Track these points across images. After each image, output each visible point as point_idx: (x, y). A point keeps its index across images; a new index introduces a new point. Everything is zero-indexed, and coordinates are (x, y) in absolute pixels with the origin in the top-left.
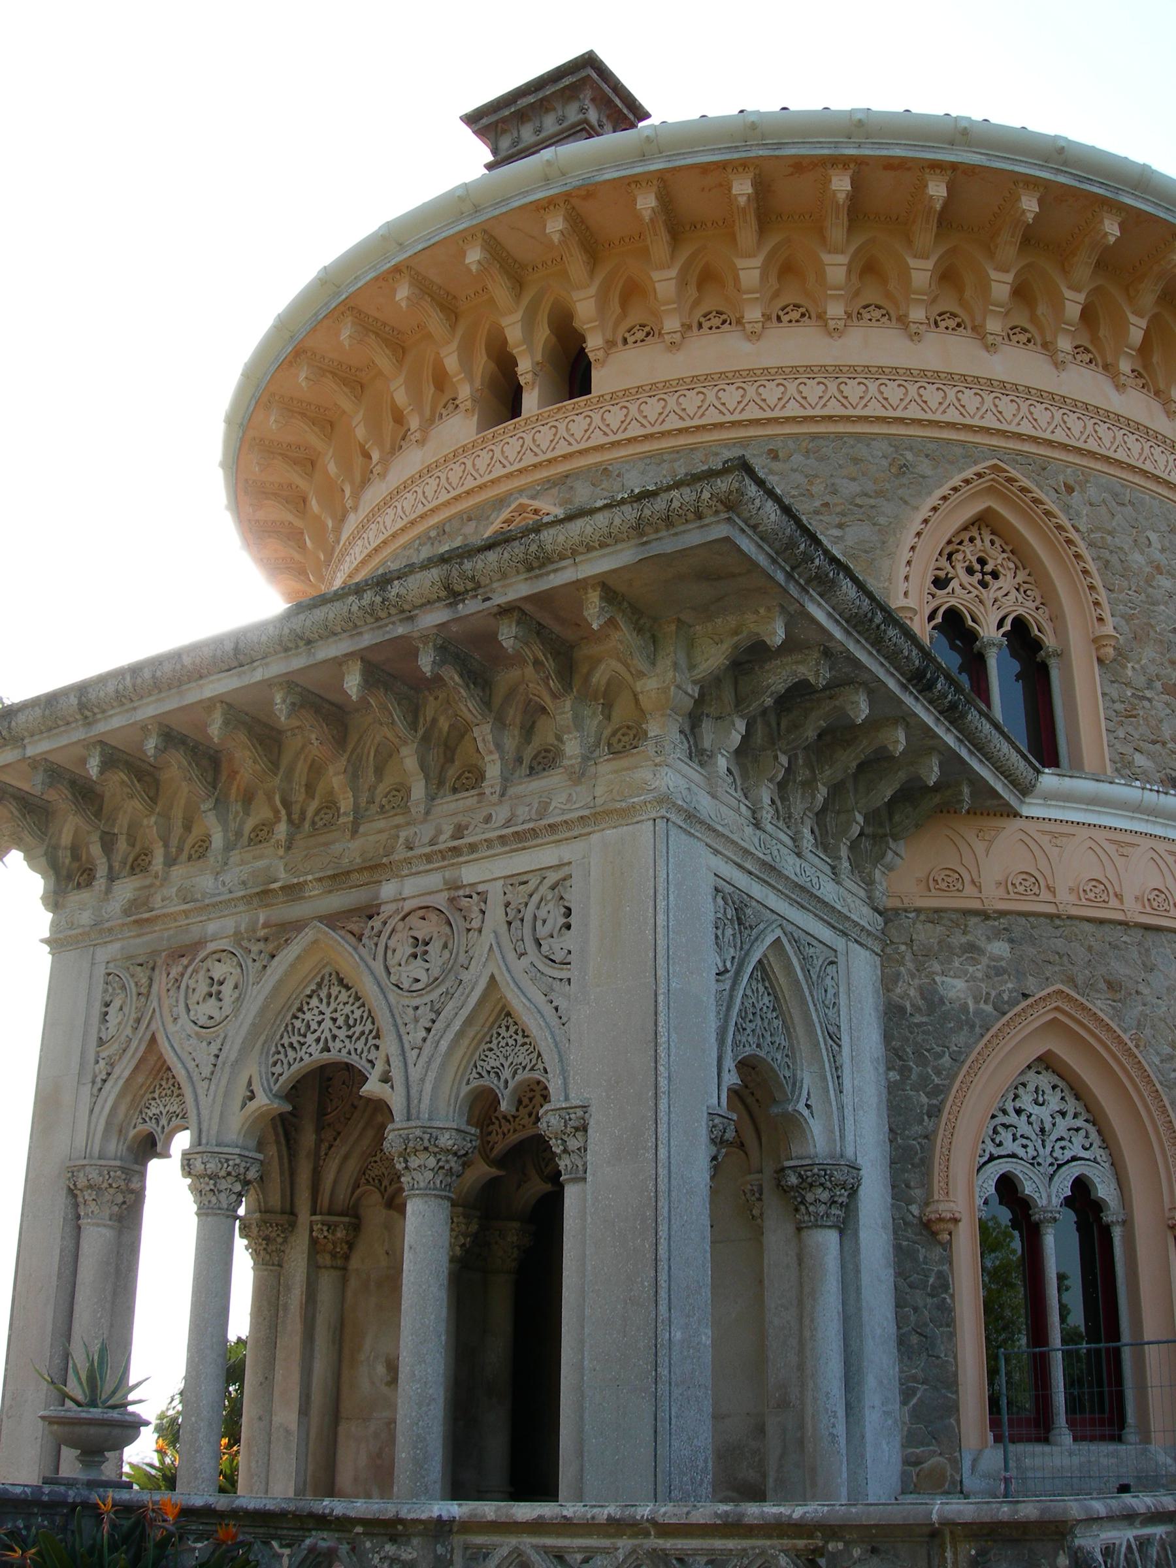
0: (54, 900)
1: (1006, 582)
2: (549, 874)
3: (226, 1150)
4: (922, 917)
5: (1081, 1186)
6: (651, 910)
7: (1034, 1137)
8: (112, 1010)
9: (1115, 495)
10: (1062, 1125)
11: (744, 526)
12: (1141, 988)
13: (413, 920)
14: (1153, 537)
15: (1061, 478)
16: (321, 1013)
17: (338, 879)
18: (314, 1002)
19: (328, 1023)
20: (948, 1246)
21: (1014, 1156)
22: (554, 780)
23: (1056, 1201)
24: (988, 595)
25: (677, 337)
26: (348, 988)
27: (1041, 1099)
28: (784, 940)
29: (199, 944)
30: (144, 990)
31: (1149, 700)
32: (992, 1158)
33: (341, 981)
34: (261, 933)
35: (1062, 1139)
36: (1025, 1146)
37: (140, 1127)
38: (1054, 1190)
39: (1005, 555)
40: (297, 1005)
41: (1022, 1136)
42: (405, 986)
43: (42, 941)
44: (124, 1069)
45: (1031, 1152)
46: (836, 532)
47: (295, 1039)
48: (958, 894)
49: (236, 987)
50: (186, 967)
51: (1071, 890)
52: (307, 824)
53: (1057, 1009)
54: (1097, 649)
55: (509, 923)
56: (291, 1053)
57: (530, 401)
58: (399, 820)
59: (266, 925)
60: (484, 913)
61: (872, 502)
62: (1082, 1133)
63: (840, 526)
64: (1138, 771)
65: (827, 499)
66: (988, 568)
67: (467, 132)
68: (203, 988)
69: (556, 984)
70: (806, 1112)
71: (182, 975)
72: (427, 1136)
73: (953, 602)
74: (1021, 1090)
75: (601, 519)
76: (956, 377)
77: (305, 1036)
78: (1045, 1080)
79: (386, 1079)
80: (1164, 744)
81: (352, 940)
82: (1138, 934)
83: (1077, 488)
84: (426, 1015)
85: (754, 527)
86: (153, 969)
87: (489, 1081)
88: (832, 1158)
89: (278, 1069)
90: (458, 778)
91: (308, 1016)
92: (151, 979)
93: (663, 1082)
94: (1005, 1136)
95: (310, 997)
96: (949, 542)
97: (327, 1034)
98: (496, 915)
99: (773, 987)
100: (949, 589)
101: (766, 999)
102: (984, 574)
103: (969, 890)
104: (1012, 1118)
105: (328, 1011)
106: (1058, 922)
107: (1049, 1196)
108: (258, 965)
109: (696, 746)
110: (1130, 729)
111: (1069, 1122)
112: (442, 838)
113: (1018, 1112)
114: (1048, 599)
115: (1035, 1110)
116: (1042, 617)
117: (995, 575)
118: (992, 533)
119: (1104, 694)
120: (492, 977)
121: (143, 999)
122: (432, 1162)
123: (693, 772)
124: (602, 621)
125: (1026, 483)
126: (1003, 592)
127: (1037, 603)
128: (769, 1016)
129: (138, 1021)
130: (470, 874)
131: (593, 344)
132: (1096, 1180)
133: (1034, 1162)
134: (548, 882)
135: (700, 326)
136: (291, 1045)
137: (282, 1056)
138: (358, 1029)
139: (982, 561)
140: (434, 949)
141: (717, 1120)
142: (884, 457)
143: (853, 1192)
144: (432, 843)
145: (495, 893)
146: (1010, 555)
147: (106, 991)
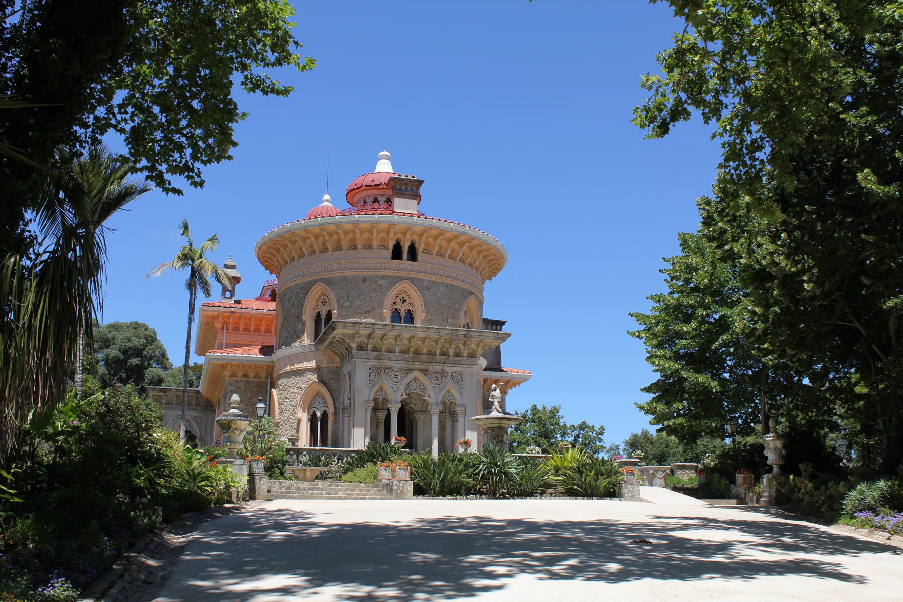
8: (372, 375)
145: (450, 373)
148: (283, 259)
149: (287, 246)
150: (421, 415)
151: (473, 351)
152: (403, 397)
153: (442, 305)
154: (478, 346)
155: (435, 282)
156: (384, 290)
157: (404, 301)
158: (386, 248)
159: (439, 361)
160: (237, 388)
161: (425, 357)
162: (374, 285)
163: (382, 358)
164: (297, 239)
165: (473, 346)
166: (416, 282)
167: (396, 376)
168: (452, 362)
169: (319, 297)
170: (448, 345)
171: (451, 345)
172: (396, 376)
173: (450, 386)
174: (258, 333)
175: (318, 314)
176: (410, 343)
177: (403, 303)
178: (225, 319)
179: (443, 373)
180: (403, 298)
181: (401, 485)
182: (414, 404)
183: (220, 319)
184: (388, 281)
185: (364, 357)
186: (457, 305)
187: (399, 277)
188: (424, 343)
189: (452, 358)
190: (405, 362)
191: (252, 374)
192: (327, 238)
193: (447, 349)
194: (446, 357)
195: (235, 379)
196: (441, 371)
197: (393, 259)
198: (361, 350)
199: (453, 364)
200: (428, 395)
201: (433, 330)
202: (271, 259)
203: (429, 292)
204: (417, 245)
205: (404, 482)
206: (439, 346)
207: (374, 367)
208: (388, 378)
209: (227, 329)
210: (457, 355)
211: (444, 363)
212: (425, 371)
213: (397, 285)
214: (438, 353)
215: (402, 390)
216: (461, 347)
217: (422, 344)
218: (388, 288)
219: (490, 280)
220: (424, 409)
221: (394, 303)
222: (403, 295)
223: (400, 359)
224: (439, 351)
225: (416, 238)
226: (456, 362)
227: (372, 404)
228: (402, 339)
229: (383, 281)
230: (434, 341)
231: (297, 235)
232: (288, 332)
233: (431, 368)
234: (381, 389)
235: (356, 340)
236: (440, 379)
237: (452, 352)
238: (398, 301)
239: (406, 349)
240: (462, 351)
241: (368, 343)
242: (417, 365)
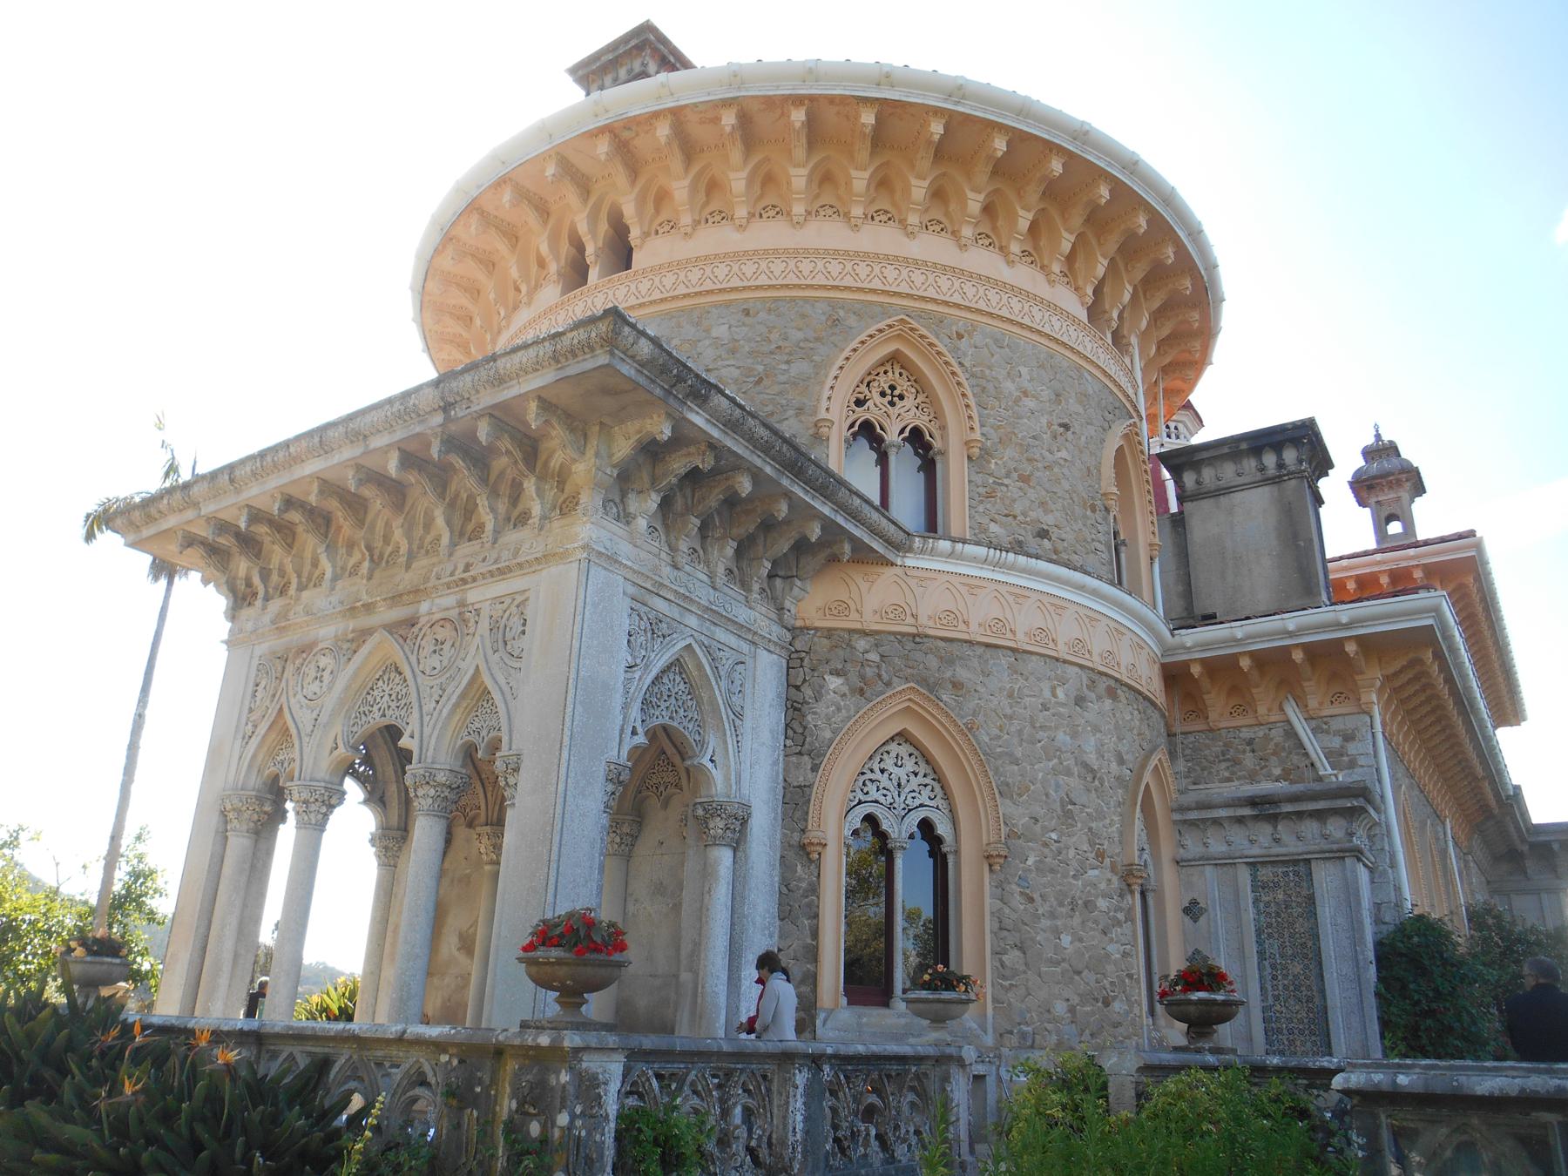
0: (232, 615)
1: (909, 402)
2: (516, 596)
3: (314, 784)
4: (819, 634)
5: (926, 826)
6: (571, 621)
7: (892, 789)
8: (260, 688)
9: (996, 341)
10: (915, 781)
11: (622, 356)
12: (979, 688)
13: (437, 628)
14: (1024, 370)
15: (954, 328)
16: (384, 691)
17: (395, 599)
18: (380, 683)
20: (818, 864)
21: (876, 802)
22: (524, 534)
23: (905, 835)
24: (893, 411)
25: (689, 230)
26: (400, 674)
27: (900, 763)
28: (695, 646)
29: (314, 644)
30: (279, 675)
31: (1007, 486)
32: (860, 802)
33: (397, 668)
34: (350, 636)
35: (914, 791)
36: (885, 796)
37: (272, 769)
38: (904, 827)
39: (909, 383)
40: (370, 685)
41: (884, 788)
42: (427, 673)
43: (223, 642)
44: (263, 728)
45: (890, 800)
46: (784, 367)
47: (366, 709)
48: (845, 618)
49: (332, 673)
50: (305, 660)
51: (930, 617)
52: (384, 564)
53: (910, 700)
54: (968, 449)
55: (491, 630)
57: (593, 275)
58: (435, 560)
59: (353, 631)
60: (477, 623)
61: (811, 345)
62: (929, 788)
63: (788, 362)
64: (992, 535)
65: (780, 343)
66: (896, 392)
67: (569, 79)
68: (313, 674)
69: (513, 671)
70: (710, 765)
71: (302, 665)
72: (427, 774)
73: (868, 416)
74: (885, 756)
75: (532, 352)
76: (881, 257)
77: (372, 706)
78: (904, 750)
80: (1015, 517)
81: (401, 640)
82: (980, 650)
83: (966, 335)
84: (437, 692)
85: (632, 357)
86: (286, 661)
87: (474, 738)
88: (729, 797)
89: (355, 729)
90: (473, 532)
91: (376, 693)
92: (284, 668)
93: (566, 740)
94: (871, 788)
95: (378, 680)
96: (870, 374)
97: (385, 705)
98: (484, 625)
99: (689, 678)
100: (866, 407)
101: (682, 686)
102: (893, 396)
103: (854, 615)
104: (878, 775)
105: (387, 690)
106: (918, 639)
107: (900, 832)
108: (346, 657)
109: (624, 510)
110: (988, 506)
111: (920, 779)
112: (457, 573)
113: (882, 771)
114: (938, 416)
115: (892, 769)
116: (933, 427)
117: (901, 397)
118: (902, 367)
119: (970, 482)
120: (477, 666)
122: (432, 792)
123: (618, 529)
124: (538, 423)
125: (924, 331)
126: (906, 409)
127: (931, 417)
128: (684, 698)
129: (274, 695)
130: (473, 596)
131: (634, 234)
132: (937, 821)
133: (891, 807)
134: (516, 603)
135: (707, 221)
136: (364, 713)
137: (358, 720)
139: (892, 388)
140: (447, 646)
141: (612, 767)
142: (824, 313)
143: (744, 822)
144: (452, 574)
146: (914, 384)
147: (257, 675)
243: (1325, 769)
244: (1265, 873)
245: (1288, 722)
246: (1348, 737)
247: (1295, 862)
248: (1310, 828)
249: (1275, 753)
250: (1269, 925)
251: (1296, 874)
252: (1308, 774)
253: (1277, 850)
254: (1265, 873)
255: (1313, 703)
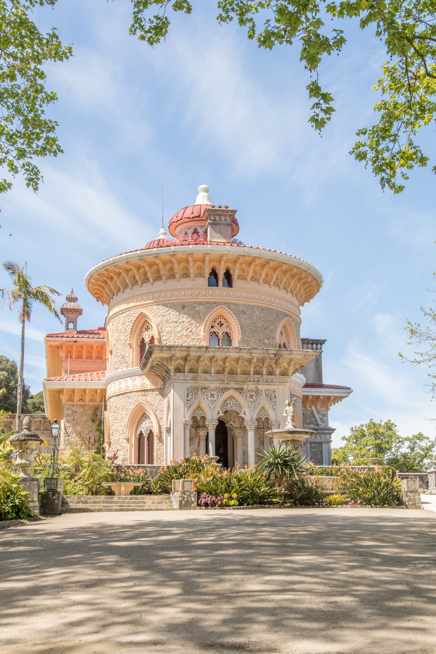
8: (189, 395)
13: (250, 392)
18: (228, 400)
19: (231, 404)
29: (209, 387)
34: (221, 388)
56: (225, 408)
68: (210, 395)
79: (244, 414)
84: (253, 406)
89: (222, 409)
98: (264, 394)
121: (196, 395)
138: (237, 405)
145: (264, 391)
148: (110, 290)
149: (112, 278)
150: (240, 431)
151: (285, 369)
152: (219, 415)
153: (258, 326)
154: (289, 364)
155: (250, 306)
156: (201, 315)
157: (222, 325)
158: (202, 276)
159: (252, 380)
160: (72, 413)
161: (240, 377)
162: (192, 311)
163: (199, 379)
164: (121, 271)
165: (285, 365)
166: (232, 307)
167: (212, 396)
168: (265, 380)
169: (143, 325)
170: (261, 365)
171: (263, 365)
172: (212, 396)
173: (263, 401)
174: (91, 360)
175: (143, 340)
176: (224, 364)
177: (220, 326)
178: (69, 348)
179: (257, 391)
180: (220, 322)
181: (186, 496)
182: (234, 422)
183: (64, 349)
184: (205, 307)
185: (182, 378)
186: (272, 327)
187: (215, 303)
188: (238, 363)
189: (265, 376)
190: (221, 382)
191: (87, 398)
192: (147, 268)
193: (260, 368)
194: (260, 376)
195: (72, 403)
196: (254, 390)
197: (209, 286)
198: (179, 372)
199: (266, 382)
200: (243, 412)
201: (245, 351)
202: (100, 291)
203: (245, 316)
204: (231, 272)
205: (188, 493)
206: (253, 365)
207: (192, 388)
208: (205, 397)
209: (71, 357)
210: (270, 373)
211: (258, 381)
212: (240, 390)
213: (214, 310)
214: (252, 373)
215: (218, 408)
216: (274, 366)
217: (236, 365)
218: (206, 313)
219: (309, 302)
220: (242, 426)
221: (212, 327)
222: (220, 320)
223: (215, 379)
224: (252, 370)
225: (230, 265)
226: (269, 381)
227: (191, 422)
228: (217, 361)
229: (201, 307)
230: (247, 361)
231: (120, 268)
232: (116, 358)
233: (245, 387)
234: (199, 407)
235: (173, 363)
236: (254, 397)
237: (265, 371)
238: (216, 325)
239: (221, 369)
240: (274, 370)
241: (184, 365)
242: (233, 385)
243: (319, 422)
244: (313, 445)
245: (312, 411)
246: (324, 416)
247: (319, 443)
248: (323, 436)
249: (308, 417)
250: (313, 456)
251: (319, 445)
252: (315, 423)
253: (316, 440)
254: (313, 445)
255: (318, 407)
